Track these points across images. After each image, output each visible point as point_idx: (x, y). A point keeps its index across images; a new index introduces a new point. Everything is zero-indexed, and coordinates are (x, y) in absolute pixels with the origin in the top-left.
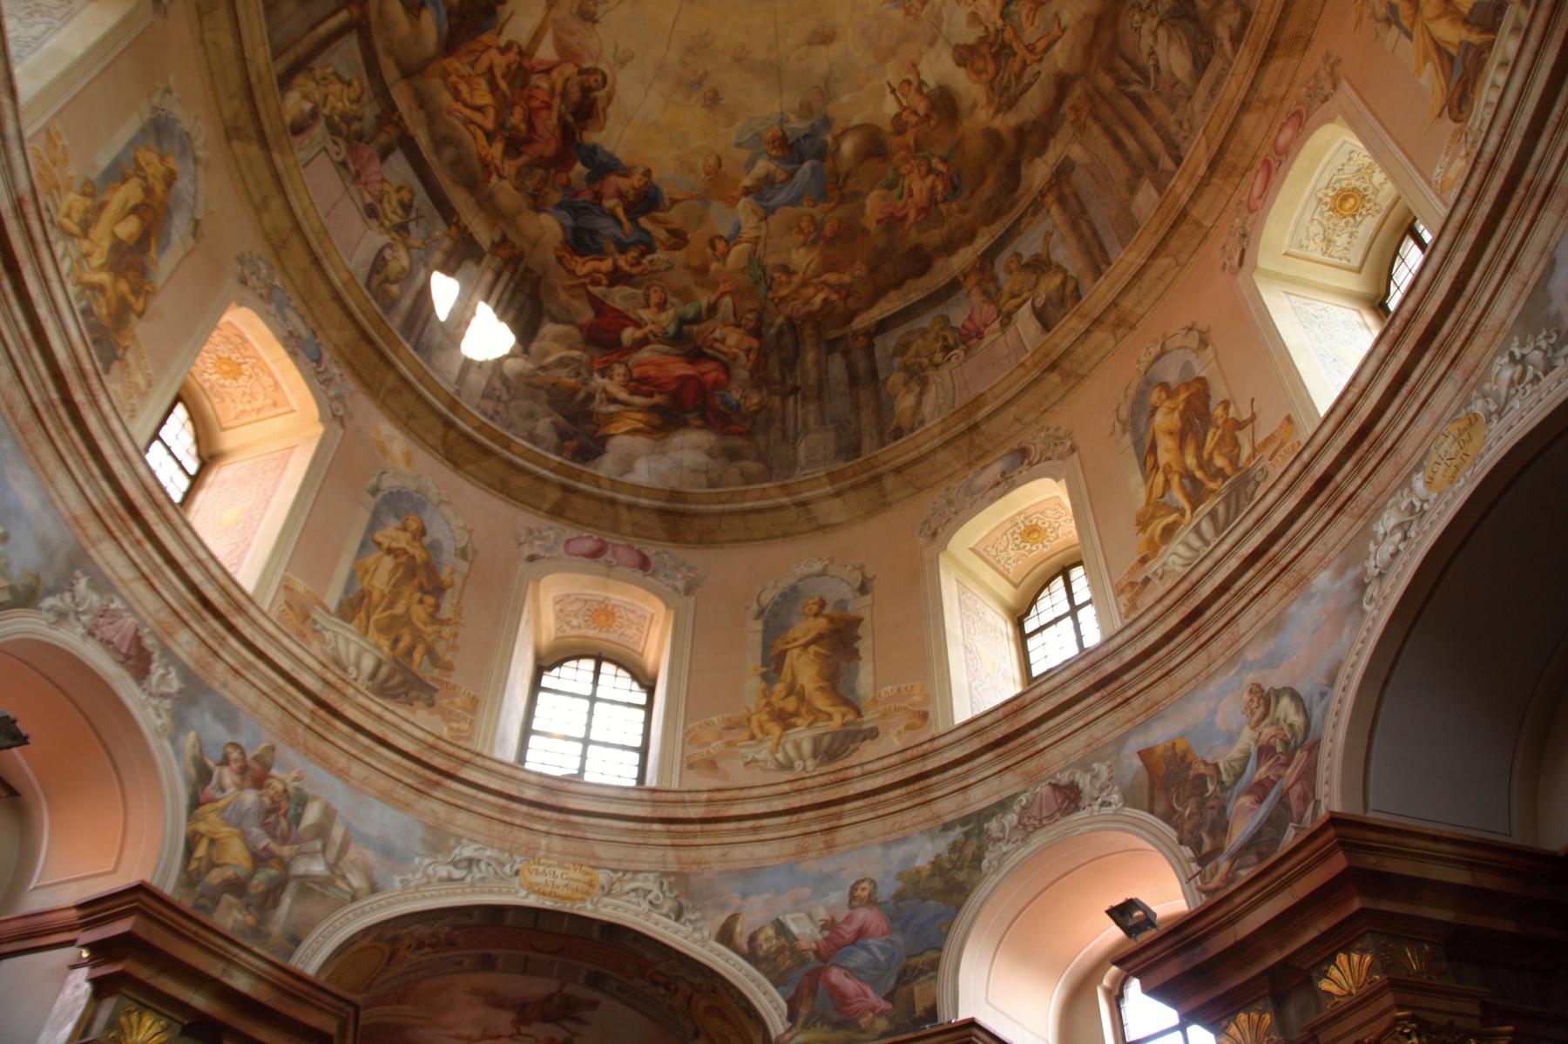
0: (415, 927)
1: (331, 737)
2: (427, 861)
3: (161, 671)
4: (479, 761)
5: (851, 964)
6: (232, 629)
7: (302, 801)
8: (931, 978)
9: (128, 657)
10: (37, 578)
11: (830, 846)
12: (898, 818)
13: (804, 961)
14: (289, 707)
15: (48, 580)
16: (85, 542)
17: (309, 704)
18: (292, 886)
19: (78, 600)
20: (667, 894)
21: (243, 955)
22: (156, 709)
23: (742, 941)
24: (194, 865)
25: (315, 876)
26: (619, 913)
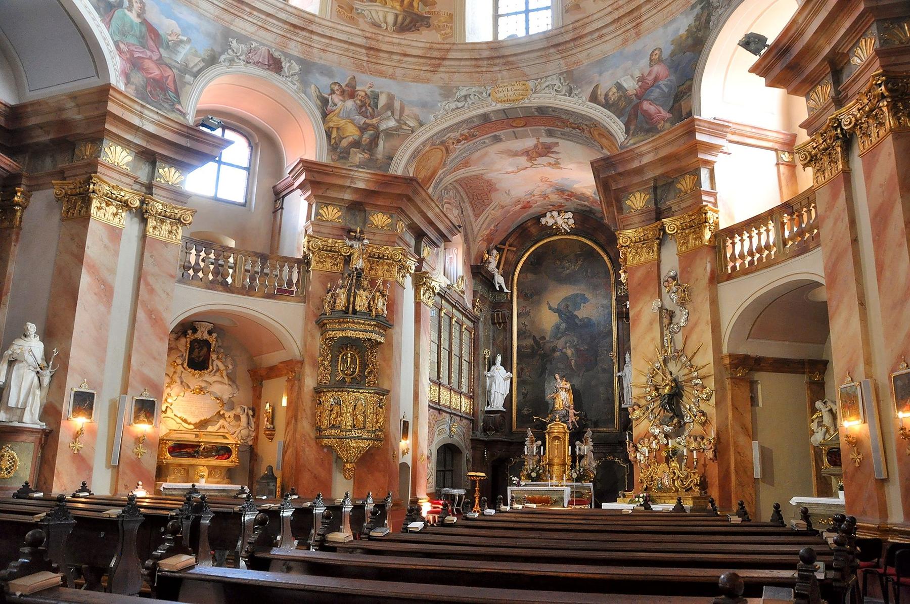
0: (449, 135)
1: (380, 62)
2: (444, 104)
3: (288, 65)
4: (455, 47)
5: (652, 97)
6: (312, 32)
7: (376, 97)
8: (689, 96)
9: (269, 65)
10: (212, 50)
11: (638, 35)
12: (669, 8)
13: (631, 101)
14: (354, 56)
15: (218, 49)
16: (227, 25)
17: (364, 51)
18: (382, 135)
19: (235, 51)
20: (564, 84)
21: (356, 174)
22: (292, 82)
23: (602, 99)
24: (333, 141)
25: (392, 128)
26: (542, 100)
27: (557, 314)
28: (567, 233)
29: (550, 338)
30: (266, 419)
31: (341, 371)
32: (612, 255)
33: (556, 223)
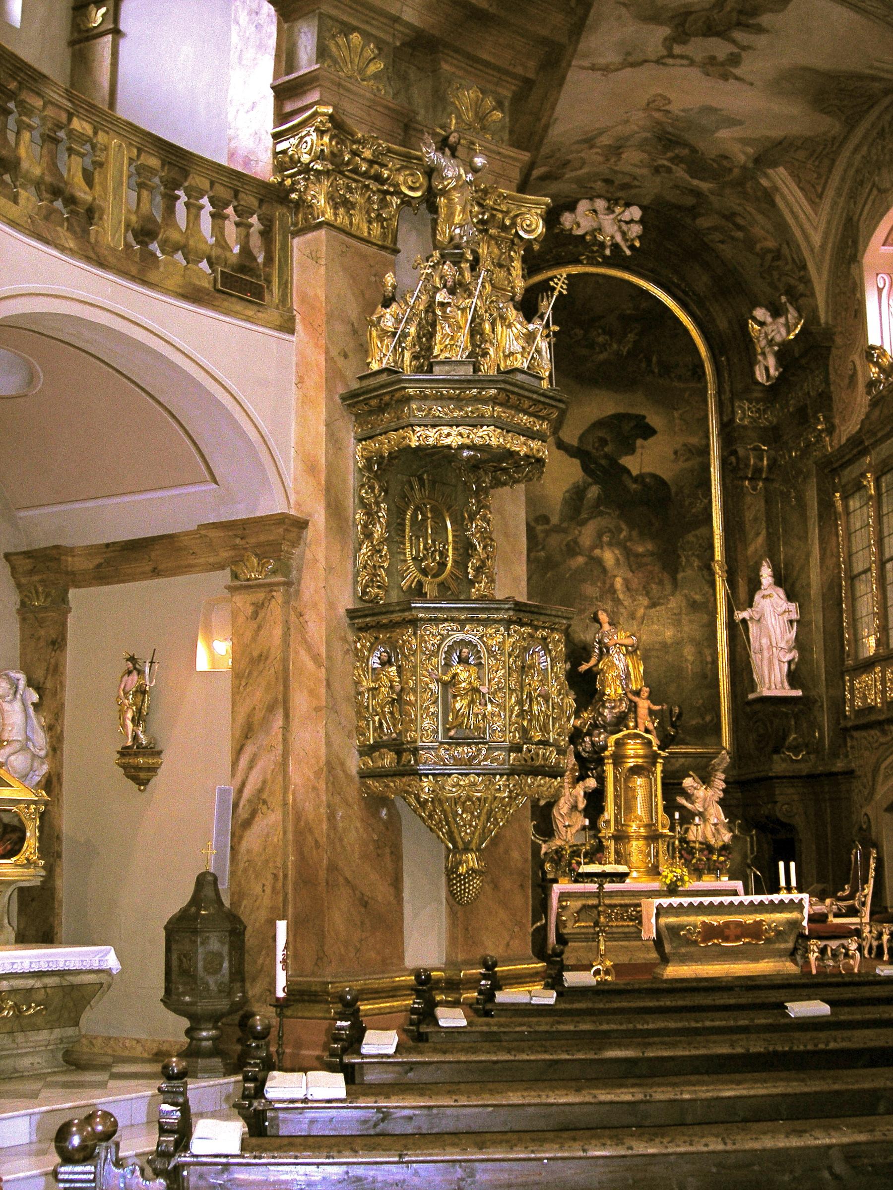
27: (577, 462)
28: (617, 259)
29: (562, 520)
30: (129, 715)
31: (413, 559)
32: (722, 324)
33: (600, 230)
